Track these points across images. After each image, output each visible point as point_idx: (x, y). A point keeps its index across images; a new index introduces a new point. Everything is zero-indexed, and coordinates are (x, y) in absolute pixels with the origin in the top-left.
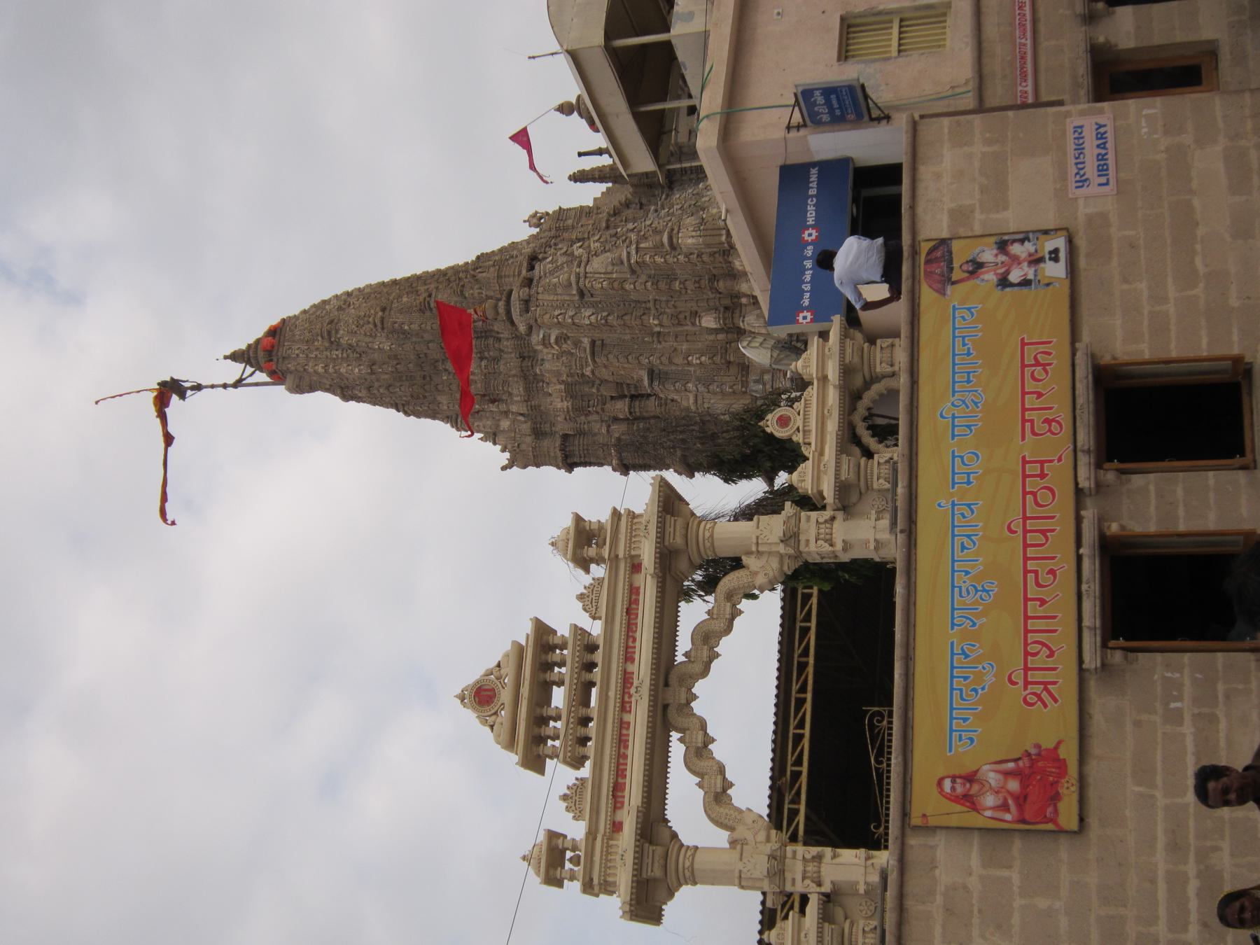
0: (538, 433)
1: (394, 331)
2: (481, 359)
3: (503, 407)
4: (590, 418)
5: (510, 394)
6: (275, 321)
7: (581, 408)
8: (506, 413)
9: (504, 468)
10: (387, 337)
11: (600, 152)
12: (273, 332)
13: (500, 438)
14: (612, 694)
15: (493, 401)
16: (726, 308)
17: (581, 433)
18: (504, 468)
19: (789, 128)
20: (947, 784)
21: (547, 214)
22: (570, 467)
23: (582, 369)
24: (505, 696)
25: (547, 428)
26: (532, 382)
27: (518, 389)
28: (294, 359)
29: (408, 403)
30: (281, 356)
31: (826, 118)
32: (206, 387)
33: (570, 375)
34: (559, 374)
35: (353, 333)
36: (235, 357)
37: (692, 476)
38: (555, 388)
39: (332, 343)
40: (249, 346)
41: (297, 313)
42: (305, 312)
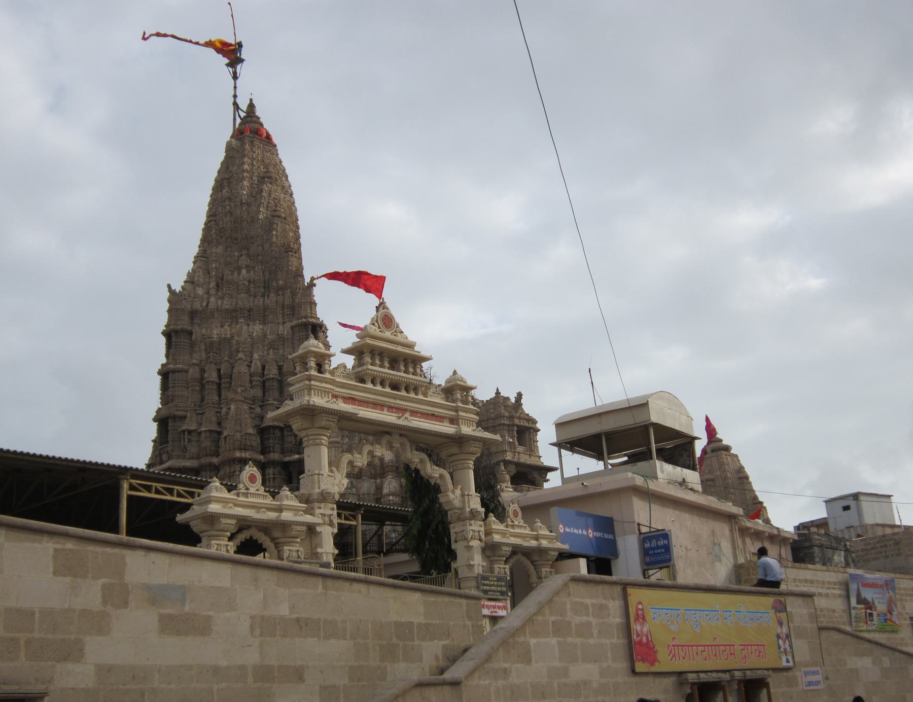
0: (193, 314)
1: (271, 224)
2: (249, 281)
3: (213, 292)
4: (203, 352)
5: (222, 298)
6: (275, 140)
7: (212, 347)
8: (208, 293)
9: (169, 286)
10: (266, 218)
13: (189, 286)
14: (398, 402)
15: (217, 285)
16: (397, 468)
17: (192, 346)
18: (169, 286)
19: (639, 524)
20: (640, 607)
21: (326, 337)
22: (169, 334)
23: (243, 351)
24: (388, 334)
25: (197, 321)
26: (232, 315)
27: (226, 304)
28: (252, 150)
29: (217, 224)
31: (647, 545)
33: (238, 343)
34: (239, 335)
35: (270, 194)
36: (251, 106)
37: (155, 420)
38: (227, 331)
40: (259, 118)
41: (280, 156)
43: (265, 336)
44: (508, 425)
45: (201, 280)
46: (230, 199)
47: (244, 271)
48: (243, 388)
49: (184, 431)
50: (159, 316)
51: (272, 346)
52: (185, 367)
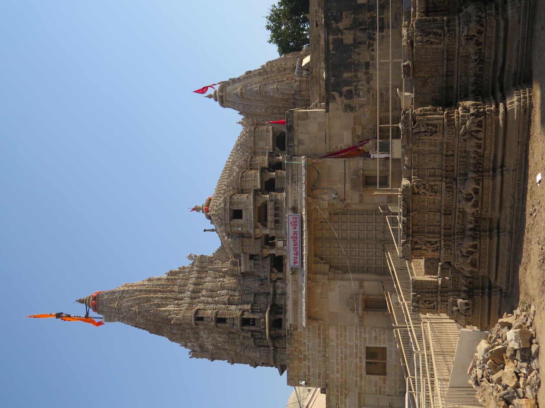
9: (190, 357)
11: (213, 230)
12: (95, 298)
18: (190, 357)
21: (195, 256)
36: (81, 301)
42: (106, 294)
44: (231, 226)
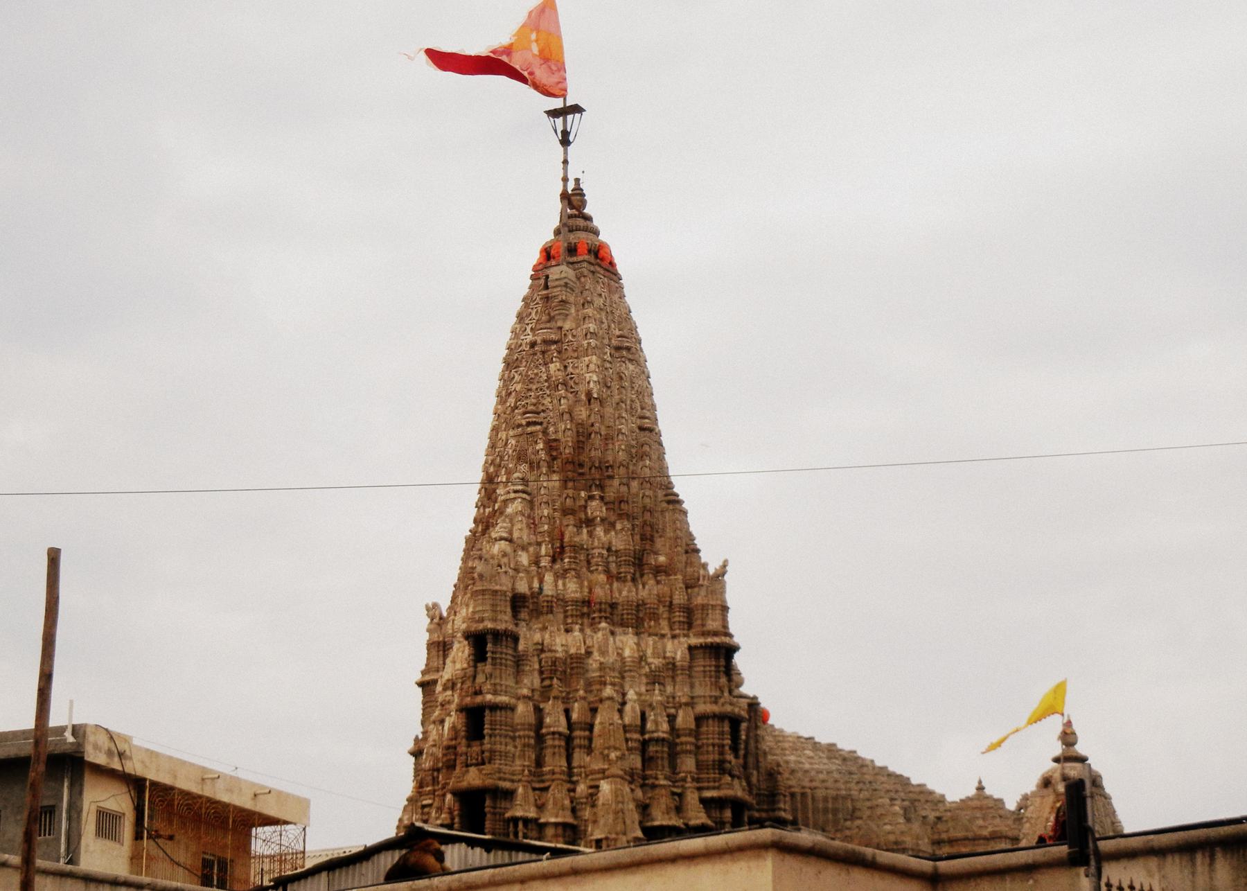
0: (517, 602)
4: (536, 674)
6: (620, 269)
17: (519, 662)
25: (524, 614)
26: (587, 611)
27: (572, 588)
30: (577, 258)
32: (566, 153)
39: (618, 348)
43: (642, 658)
45: (525, 538)
46: (565, 384)
47: (599, 531)
48: (618, 753)
49: (515, 820)
50: (906, 774)
51: (655, 679)
52: (513, 701)
